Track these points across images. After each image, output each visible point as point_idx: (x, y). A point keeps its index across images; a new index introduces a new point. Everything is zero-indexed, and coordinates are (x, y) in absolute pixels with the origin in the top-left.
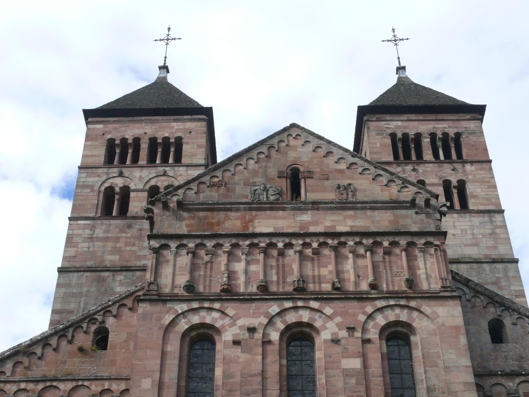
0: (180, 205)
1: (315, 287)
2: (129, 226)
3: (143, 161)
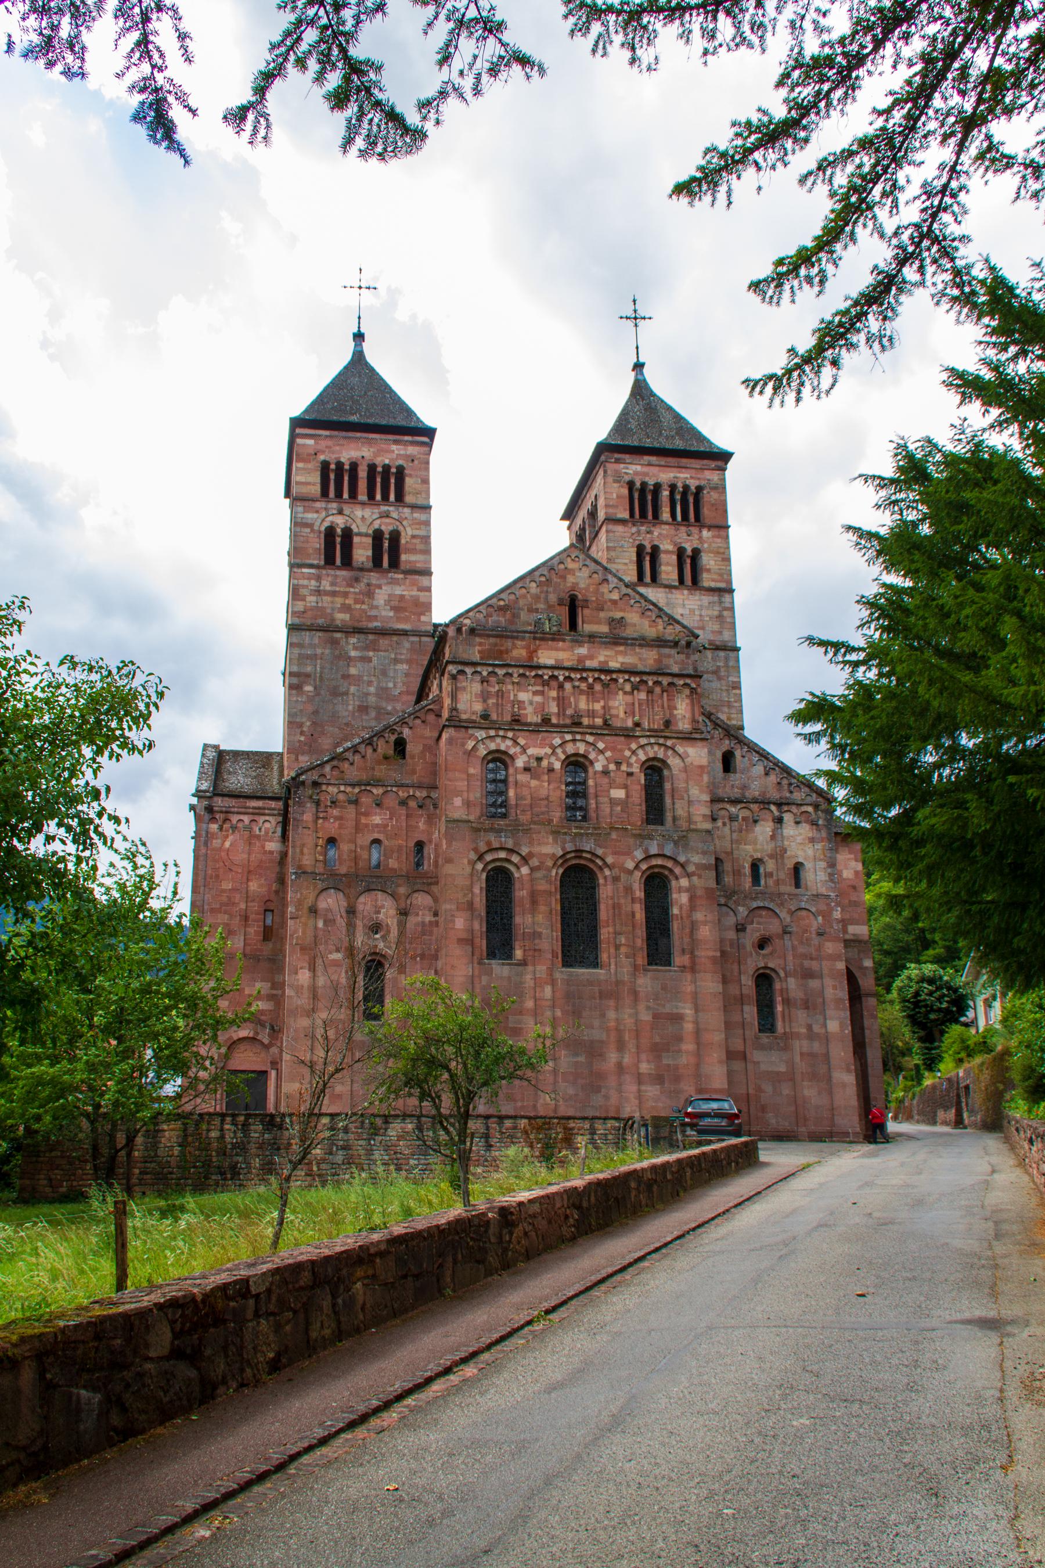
0: (472, 631)
2: (357, 580)
3: (363, 497)
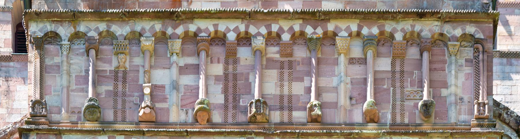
1: (282, 116)
